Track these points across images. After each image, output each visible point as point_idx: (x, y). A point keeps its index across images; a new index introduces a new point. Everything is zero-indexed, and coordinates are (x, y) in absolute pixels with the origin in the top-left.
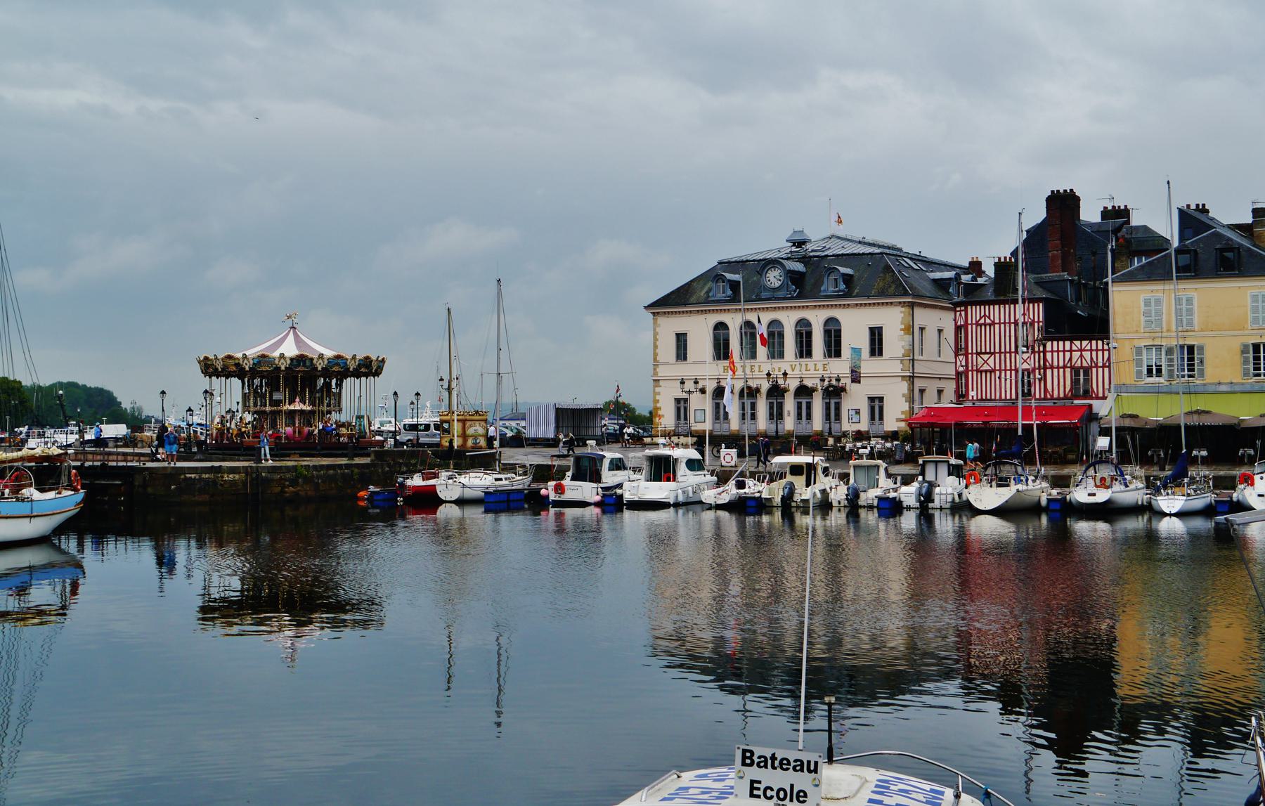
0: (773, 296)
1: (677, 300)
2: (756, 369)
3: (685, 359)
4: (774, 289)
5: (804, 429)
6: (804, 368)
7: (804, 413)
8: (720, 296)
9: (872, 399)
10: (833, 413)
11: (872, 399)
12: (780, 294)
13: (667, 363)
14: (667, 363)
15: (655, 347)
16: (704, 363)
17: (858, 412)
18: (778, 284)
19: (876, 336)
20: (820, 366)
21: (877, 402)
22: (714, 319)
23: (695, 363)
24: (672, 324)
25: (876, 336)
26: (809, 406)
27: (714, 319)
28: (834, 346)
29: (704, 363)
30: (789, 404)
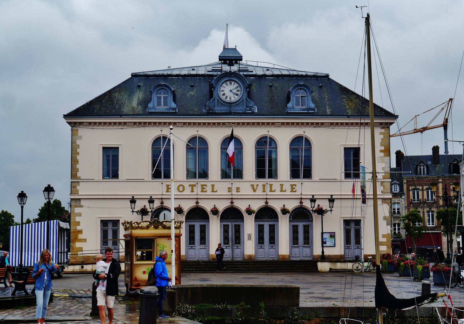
0: (230, 110)
1: (100, 109)
2: (209, 188)
3: (115, 175)
4: (230, 104)
5: (267, 253)
6: (268, 188)
7: (266, 236)
8: (162, 108)
9: (347, 222)
10: (301, 236)
11: (347, 222)
12: (239, 109)
13: (92, 181)
14: (92, 181)
15: (74, 161)
16: (142, 181)
17: (333, 235)
18: (234, 99)
19: (352, 157)
20: (287, 187)
21: (353, 226)
22: (155, 132)
23: (129, 180)
24: (96, 138)
25: (352, 157)
26: (273, 230)
27: (155, 132)
28: (302, 168)
29: (142, 181)
30: (249, 227)
